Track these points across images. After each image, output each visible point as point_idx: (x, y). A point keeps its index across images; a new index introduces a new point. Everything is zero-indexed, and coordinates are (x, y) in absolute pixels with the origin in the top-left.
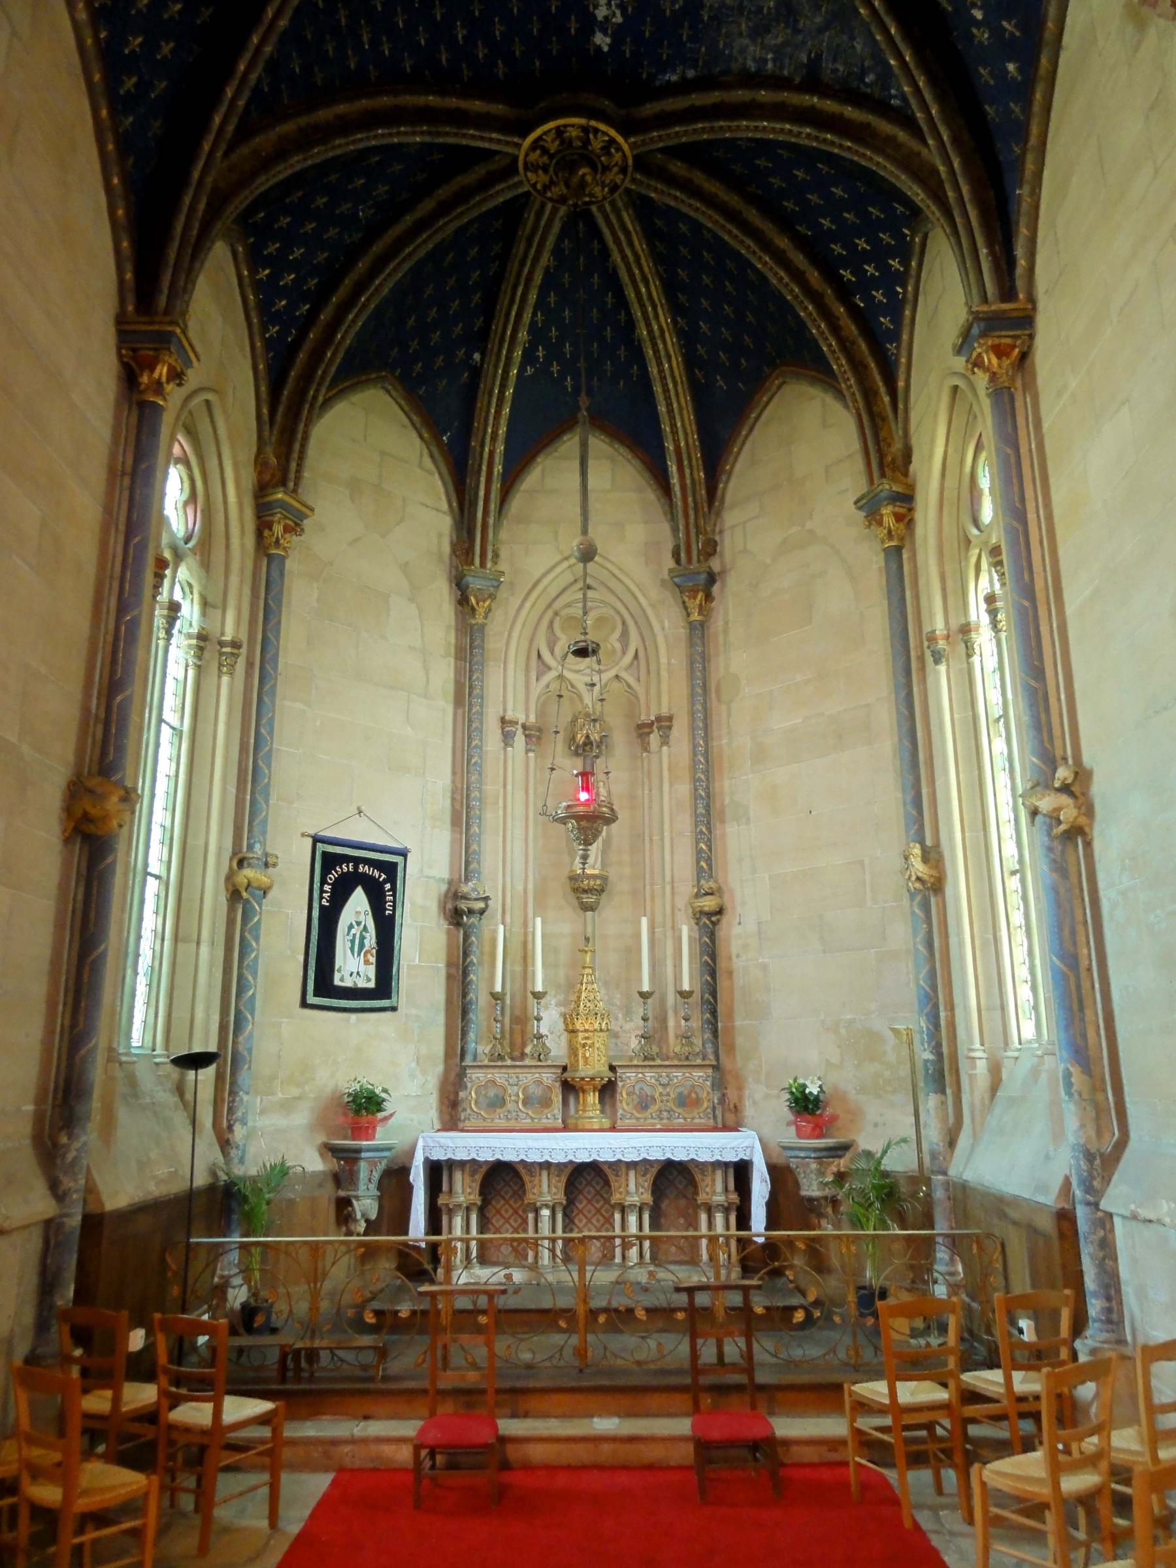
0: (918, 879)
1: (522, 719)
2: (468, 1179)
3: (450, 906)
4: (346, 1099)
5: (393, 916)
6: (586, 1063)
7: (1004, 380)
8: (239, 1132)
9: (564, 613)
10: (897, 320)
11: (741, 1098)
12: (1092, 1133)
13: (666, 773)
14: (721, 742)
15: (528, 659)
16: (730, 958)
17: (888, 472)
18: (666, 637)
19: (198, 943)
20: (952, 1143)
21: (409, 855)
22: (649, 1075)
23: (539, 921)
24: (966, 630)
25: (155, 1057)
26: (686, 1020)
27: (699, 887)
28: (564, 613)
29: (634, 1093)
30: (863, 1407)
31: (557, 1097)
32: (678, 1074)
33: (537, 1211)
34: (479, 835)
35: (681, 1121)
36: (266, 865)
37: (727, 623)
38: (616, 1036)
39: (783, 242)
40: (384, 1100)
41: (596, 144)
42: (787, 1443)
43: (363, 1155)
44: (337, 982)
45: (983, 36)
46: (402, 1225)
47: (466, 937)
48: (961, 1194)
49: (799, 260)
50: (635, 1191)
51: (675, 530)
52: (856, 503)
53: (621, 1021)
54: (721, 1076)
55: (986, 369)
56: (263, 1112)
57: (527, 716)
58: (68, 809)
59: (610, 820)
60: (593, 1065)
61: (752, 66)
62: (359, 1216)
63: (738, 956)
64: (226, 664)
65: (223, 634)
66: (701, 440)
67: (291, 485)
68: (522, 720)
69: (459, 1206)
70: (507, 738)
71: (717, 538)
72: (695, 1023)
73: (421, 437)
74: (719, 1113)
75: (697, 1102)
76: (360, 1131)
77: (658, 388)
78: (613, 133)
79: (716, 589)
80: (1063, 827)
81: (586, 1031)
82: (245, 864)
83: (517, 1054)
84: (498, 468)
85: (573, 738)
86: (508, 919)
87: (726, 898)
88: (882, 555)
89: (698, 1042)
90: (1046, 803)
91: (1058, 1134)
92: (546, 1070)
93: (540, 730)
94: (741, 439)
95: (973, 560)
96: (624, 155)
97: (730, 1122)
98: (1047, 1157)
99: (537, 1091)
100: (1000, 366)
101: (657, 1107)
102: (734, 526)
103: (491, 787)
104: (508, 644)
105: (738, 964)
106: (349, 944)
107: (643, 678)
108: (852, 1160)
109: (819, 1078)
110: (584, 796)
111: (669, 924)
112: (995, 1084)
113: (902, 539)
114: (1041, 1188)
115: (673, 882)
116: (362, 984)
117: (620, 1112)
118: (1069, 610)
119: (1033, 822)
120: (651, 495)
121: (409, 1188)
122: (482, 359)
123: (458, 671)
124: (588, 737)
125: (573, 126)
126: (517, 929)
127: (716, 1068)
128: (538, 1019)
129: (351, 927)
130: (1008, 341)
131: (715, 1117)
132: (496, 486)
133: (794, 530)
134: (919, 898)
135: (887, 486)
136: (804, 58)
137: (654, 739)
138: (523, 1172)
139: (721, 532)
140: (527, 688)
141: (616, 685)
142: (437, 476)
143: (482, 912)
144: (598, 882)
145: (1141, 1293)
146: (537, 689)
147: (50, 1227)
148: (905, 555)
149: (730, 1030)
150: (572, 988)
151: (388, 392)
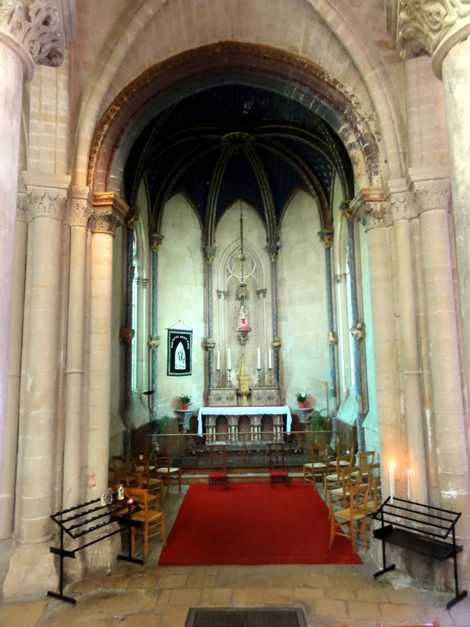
1: (223, 290)
2: (212, 419)
3: (204, 345)
4: (180, 399)
6: (243, 389)
7: (350, 220)
9: (234, 257)
10: (330, 181)
11: (285, 397)
13: (265, 306)
14: (280, 297)
15: (224, 271)
17: (327, 226)
19: (142, 361)
20: (337, 409)
21: (193, 332)
22: (260, 391)
24: (345, 275)
26: (271, 376)
28: (234, 257)
30: (308, 469)
31: (235, 397)
32: (268, 391)
33: (231, 427)
36: (158, 339)
38: (251, 380)
40: (190, 399)
41: (244, 137)
42: (291, 478)
43: (186, 414)
44: (176, 368)
46: (196, 431)
47: (209, 354)
48: (338, 422)
49: (302, 162)
50: (256, 422)
51: (267, 232)
53: (252, 376)
54: (280, 392)
55: (346, 217)
57: (224, 289)
58: (120, 336)
59: (250, 330)
60: (245, 389)
62: (185, 429)
64: (145, 285)
65: (143, 277)
66: (275, 206)
67: (158, 231)
68: (223, 290)
69: (210, 426)
70: (219, 296)
72: (273, 377)
73: (192, 206)
74: (279, 401)
75: (273, 398)
76: (185, 408)
77: (261, 192)
78: (248, 135)
80: (358, 338)
81: (243, 380)
82: (152, 339)
83: (224, 385)
84: (215, 215)
86: (220, 349)
87: (282, 342)
89: (273, 382)
90: (355, 332)
91: (355, 410)
93: (228, 293)
97: (282, 405)
99: (230, 396)
103: (215, 310)
104: (218, 268)
105: (284, 361)
106: (178, 358)
107: (258, 277)
108: (313, 414)
109: (305, 392)
110: (243, 325)
111: (266, 349)
113: (330, 245)
116: (182, 368)
120: (260, 222)
121: (197, 422)
122: (210, 184)
123: (204, 277)
126: (223, 351)
127: (279, 389)
128: (230, 376)
129: (179, 353)
131: (278, 402)
132: (214, 220)
135: (326, 231)
137: (261, 295)
138: (227, 417)
140: (224, 281)
141: (250, 279)
143: (213, 347)
146: (227, 280)
147: (125, 433)
148: (331, 249)
149: (282, 379)
150: (238, 367)
151: (182, 194)
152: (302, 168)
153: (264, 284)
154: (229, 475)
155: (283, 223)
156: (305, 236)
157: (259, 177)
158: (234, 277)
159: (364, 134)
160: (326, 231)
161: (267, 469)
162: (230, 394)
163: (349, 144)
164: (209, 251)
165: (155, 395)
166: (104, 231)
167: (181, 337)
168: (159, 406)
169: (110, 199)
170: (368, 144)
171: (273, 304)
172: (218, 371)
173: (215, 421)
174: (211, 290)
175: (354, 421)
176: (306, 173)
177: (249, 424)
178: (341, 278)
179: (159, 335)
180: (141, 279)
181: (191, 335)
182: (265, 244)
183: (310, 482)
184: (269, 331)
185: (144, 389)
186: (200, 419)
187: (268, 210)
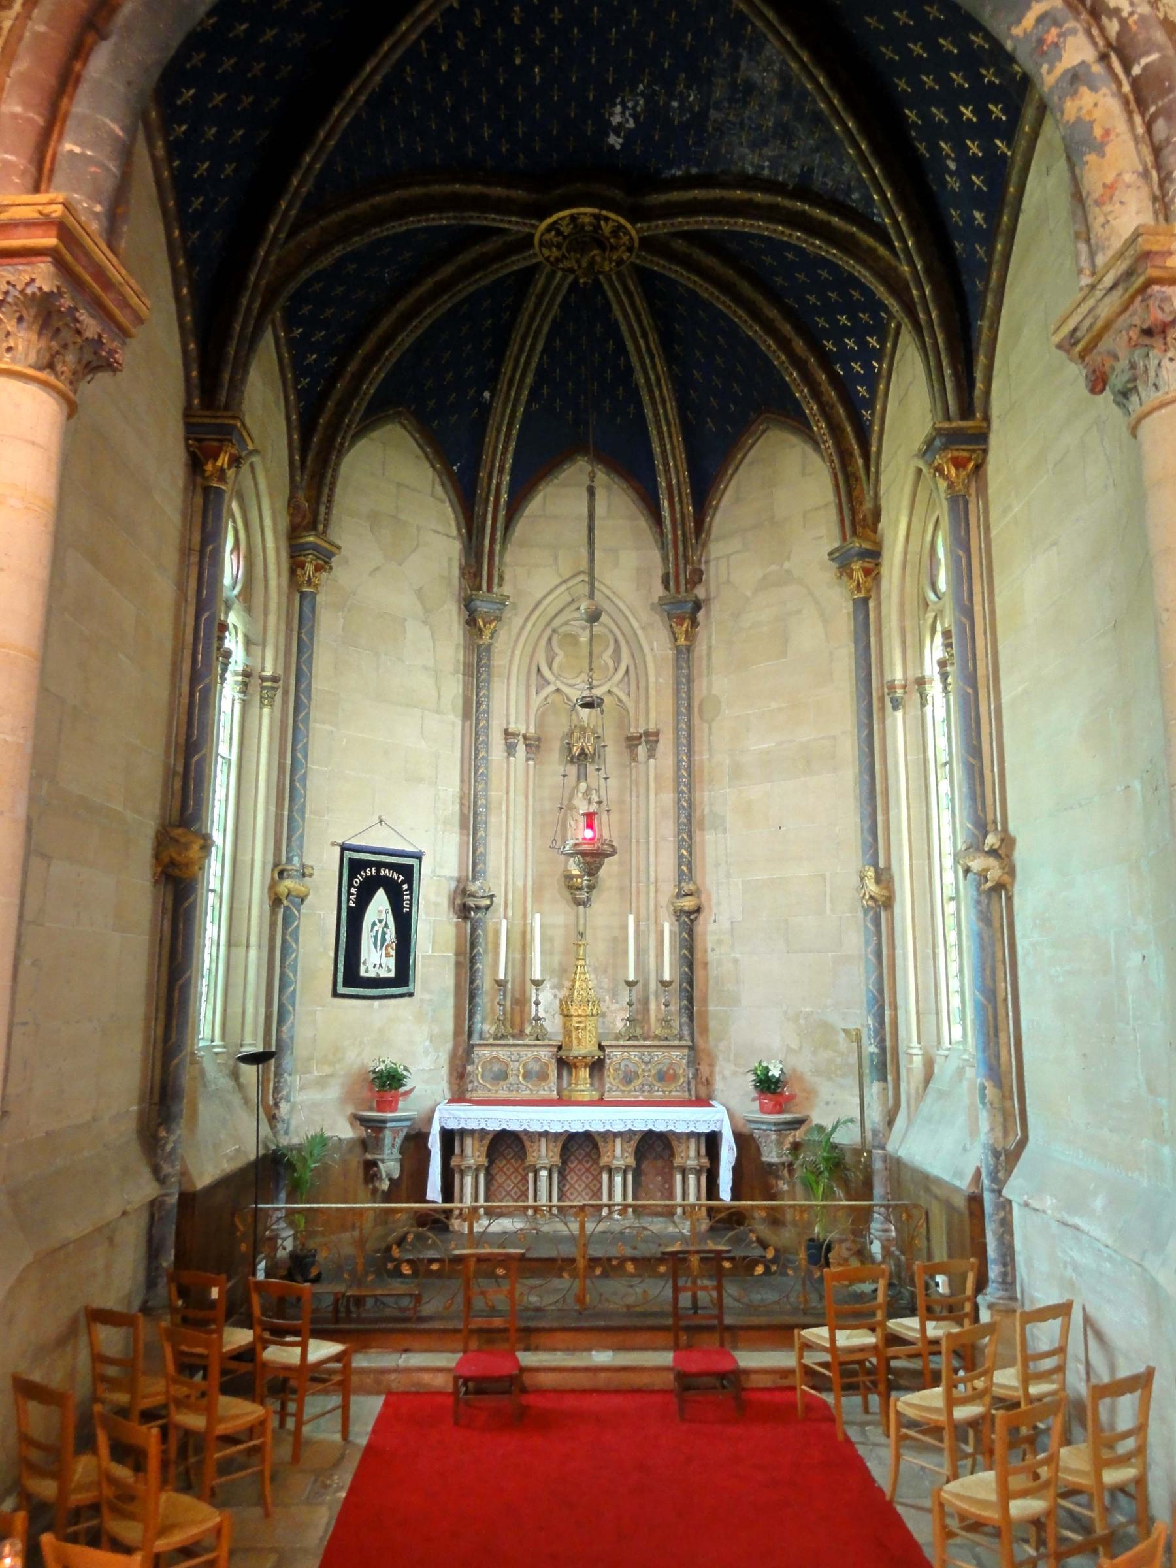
0: (871, 897)
2: (477, 1145)
3: (458, 901)
4: (372, 1076)
5: (410, 913)
7: (959, 487)
10: (873, 390)
11: (712, 1073)
12: (1000, 1134)
14: (702, 756)
15: (529, 672)
16: (706, 951)
17: (859, 530)
18: (654, 656)
19: (248, 946)
20: (890, 1123)
21: (423, 858)
23: (538, 916)
24: (921, 682)
25: (214, 1047)
26: (666, 1006)
27: (680, 889)
28: (561, 630)
29: (619, 1069)
30: (807, 1346)
31: (553, 1072)
33: (536, 1173)
36: (304, 875)
38: (604, 1015)
39: (772, 313)
40: (405, 1077)
41: (607, 228)
42: (747, 1372)
43: (389, 1125)
44: (363, 974)
45: (954, 184)
47: (474, 930)
48: (896, 1166)
49: (787, 329)
50: (620, 1156)
51: (665, 559)
52: (830, 554)
54: (696, 1057)
55: (946, 477)
57: (528, 727)
58: (157, 856)
60: (584, 1047)
61: (750, 170)
63: (713, 950)
65: (263, 670)
66: (690, 476)
67: (321, 527)
68: (523, 731)
69: (469, 1167)
70: (510, 749)
71: (703, 567)
72: (674, 1008)
73: (433, 466)
75: (674, 1077)
78: (622, 221)
79: (701, 615)
80: (989, 884)
81: (579, 1016)
82: (285, 874)
83: (516, 1031)
84: (505, 496)
85: (570, 750)
86: (510, 913)
88: (851, 602)
89: (676, 1024)
90: (977, 863)
91: (974, 1132)
93: (539, 739)
94: (728, 477)
95: (930, 621)
96: (631, 238)
97: (702, 1101)
98: (965, 1149)
99: (536, 1067)
100: (957, 475)
102: (718, 559)
105: (712, 957)
107: (632, 695)
108: (806, 1133)
109: (781, 1062)
110: (589, 834)
112: (928, 1077)
113: (868, 591)
114: (958, 1174)
116: (384, 974)
117: (608, 1085)
118: (1005, 699)
119: (965, 877)
121: (428, 1153)
122: (492, 397)
124: (583, 749)
125: (585, 214)
126: (518, 921)
127: (692, 1048)
128: (537, 1004)
129: (374, 924)
130: (965, 454)
131: (689, 1090)
132: (502, 513)
133: (774, 567)
134: (871, 914)
135: (857, 544)
136: (797, 170)
137: (642, 750)
138: (524, 1138)
139: (707, 562)
142: (447, 504)
143: (488, 908)
145: (1029, 1263)
146: (536, 701)
147: (154, 1206)
148: (871, 604)
149: (704, 1014)
150: (565, 973)
151: (405, 427)
152: (784, 344)
153: (653, 715)
154: (527, 1359)
155: (715, 531)
156: (787, 565)
157: (647, 379)
158: (558, 690)
159: (1136, 17)
160: (857, 544)
161: (662, 1338)
162: (537, 1059)
163: (1066, 72)
164: (482, 607)
165: (287, 1061)
166: (18, 368)
167: (384, 872)
168: (298, 1097)
169: (45, 223)
170: (1154, 57)
171: (677, 777)
172: (501, 984)
173: (484, 1150)
174: (487, 727)
175: (970, 1173)
176: (799, 364)
177: (596, 1162)
178: (905, 693)
179: (308, 862)
180: (256, 674)
181: (416, 870)
182: (659, 591)
183: (813, 1388)
184: (664, 864)
185: (248, 1040)
186: (435, 1144)
187: (669, 485)
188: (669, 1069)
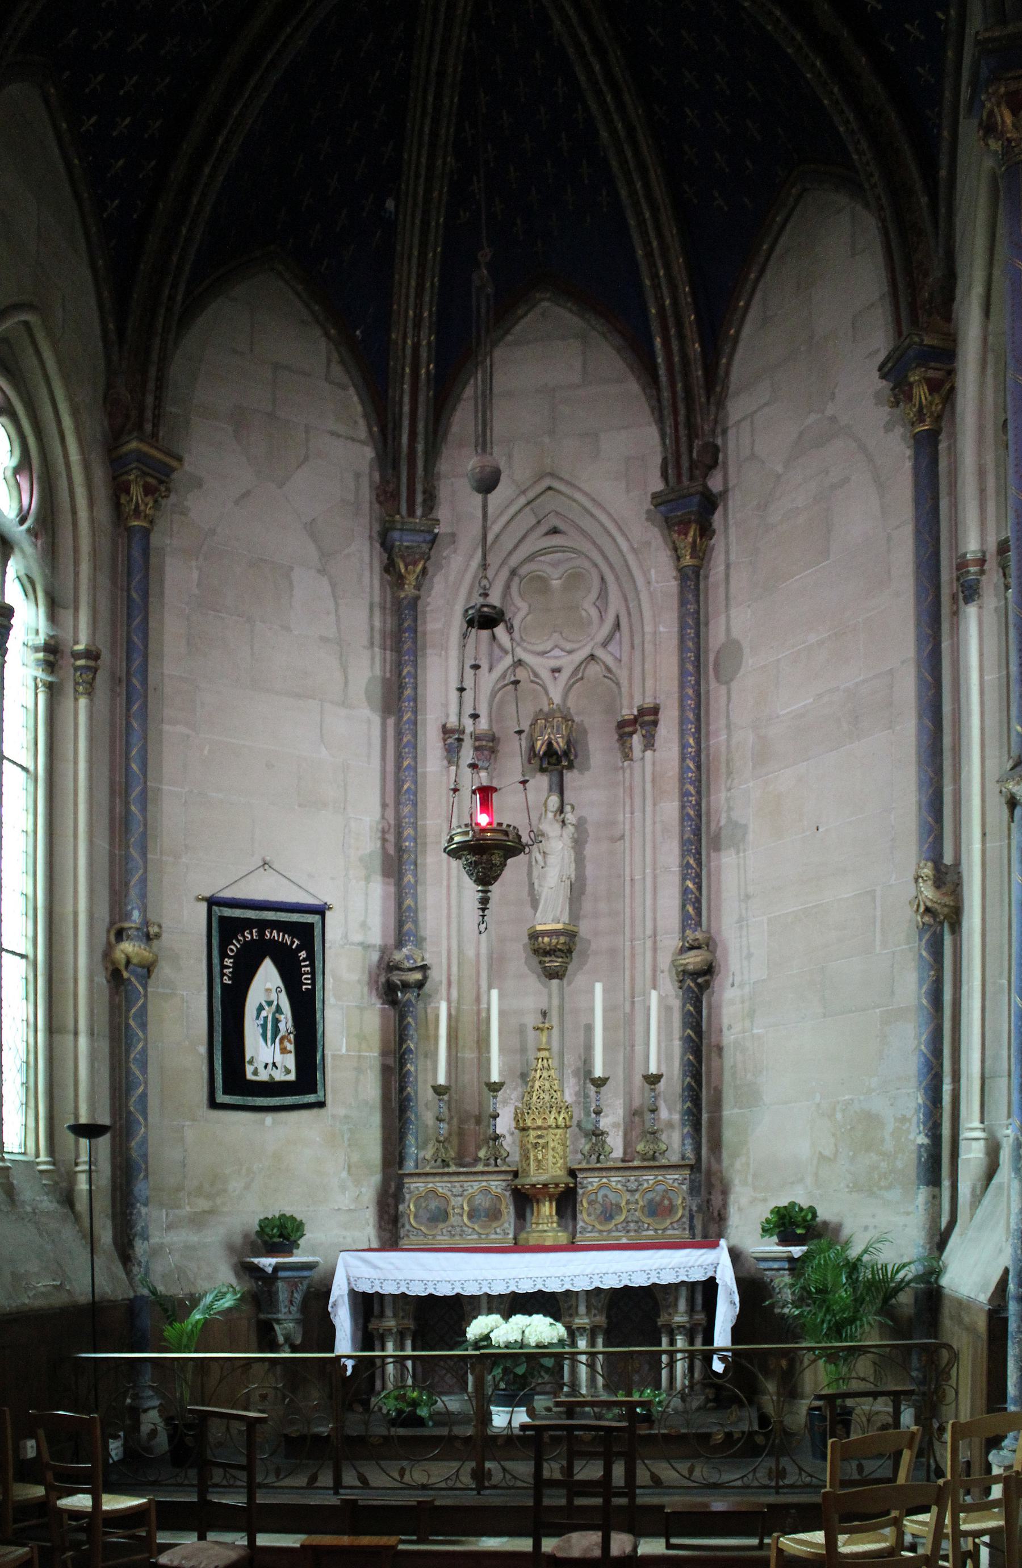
5: (312, 992)
6: (539, 1167)
8: (140, 1248)
13: (649, 786)
16: (721, 1031)
28: (523, 571)
29: (595, 1201)
34: (415, 886)
35: (651, 1233)
37: (728, 566)
56: (170, 1227)
63: (730, 1027)
81: (539, 1128)
85: (532, 747)
92: (494, 1177)
99: (484, 1202)
101: (623, 1218)
105: (729, 1038)
115: (655, 935)
124: (550, 744)
129: (261, 1008)
137: (636, 740)
142: (352, 391)
144: (562, 940)
162: (486, 1191)
164: (403, 540)
181: (317, 931)
188: (663, 1198)
